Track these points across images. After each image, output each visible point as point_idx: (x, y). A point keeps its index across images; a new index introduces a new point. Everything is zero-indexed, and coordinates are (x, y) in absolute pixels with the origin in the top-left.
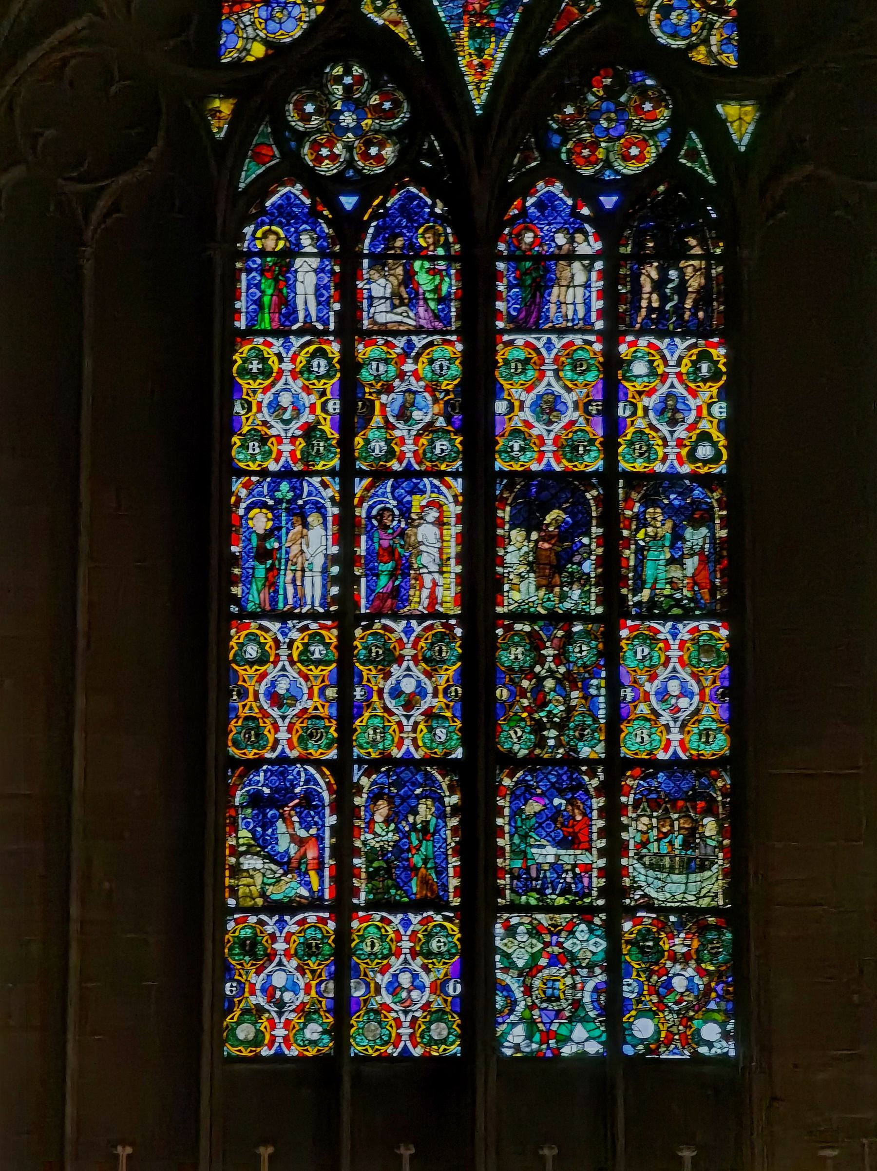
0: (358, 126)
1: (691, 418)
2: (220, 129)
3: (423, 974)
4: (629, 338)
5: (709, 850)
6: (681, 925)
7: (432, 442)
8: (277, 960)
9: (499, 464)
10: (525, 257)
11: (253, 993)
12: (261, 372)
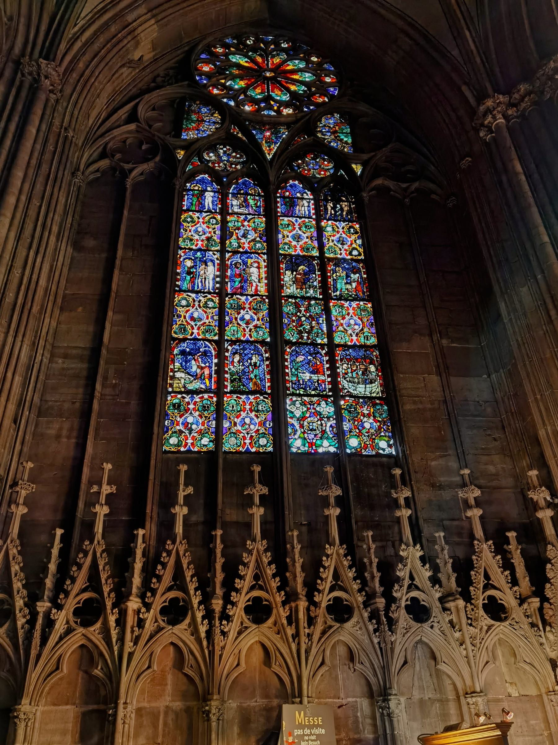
1: (349, 243)
3: (255, 418)
4: (325, 221)
5: (373, 377)
8: (190, 412)
12: (192, 221)
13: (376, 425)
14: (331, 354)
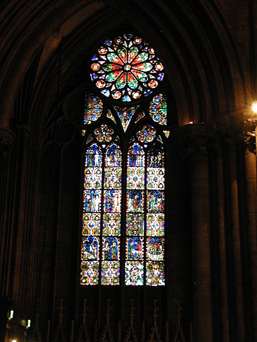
0: (106, 134)
1: (158, 181)
2: (83, 135)
5: (161, 251)
6: (156, 264)
7: (116, 185)
8: (89, 269)
9: (128, 188)
10: (132, 155)
11: (85, 274)
13: (159, 273)
14: (145, 241)
